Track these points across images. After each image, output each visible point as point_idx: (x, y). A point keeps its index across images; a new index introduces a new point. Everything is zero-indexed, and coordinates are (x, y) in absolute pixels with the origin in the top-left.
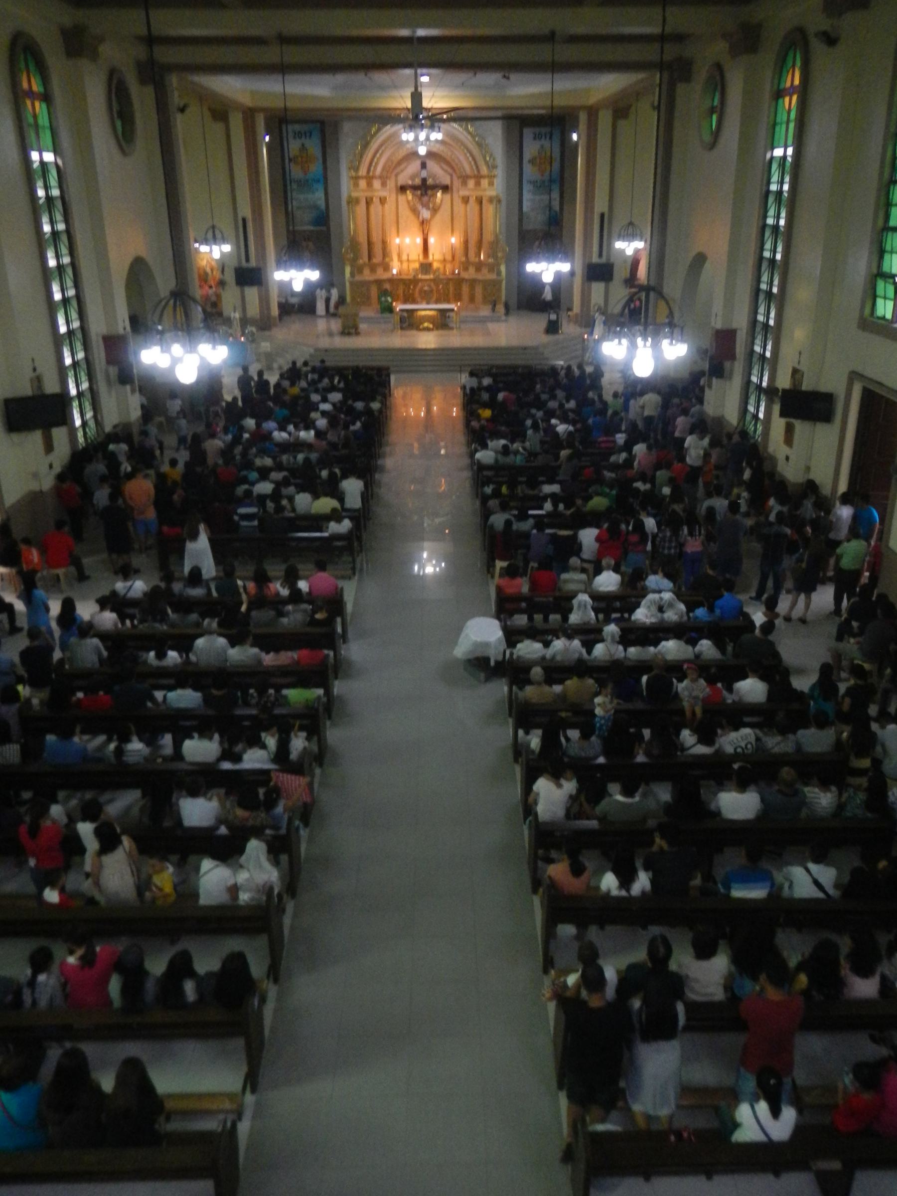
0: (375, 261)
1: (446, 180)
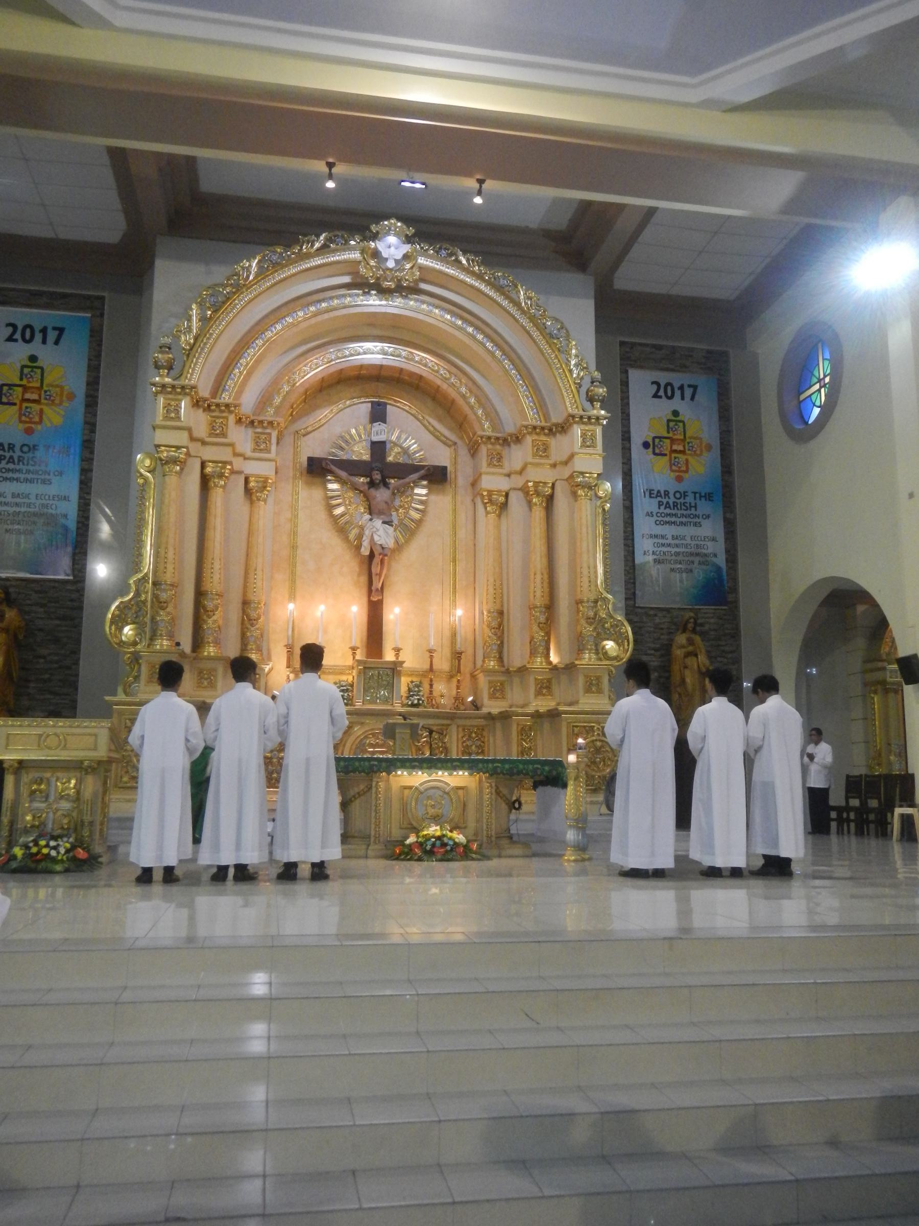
0: (210, 650)
1: (441, 456)
